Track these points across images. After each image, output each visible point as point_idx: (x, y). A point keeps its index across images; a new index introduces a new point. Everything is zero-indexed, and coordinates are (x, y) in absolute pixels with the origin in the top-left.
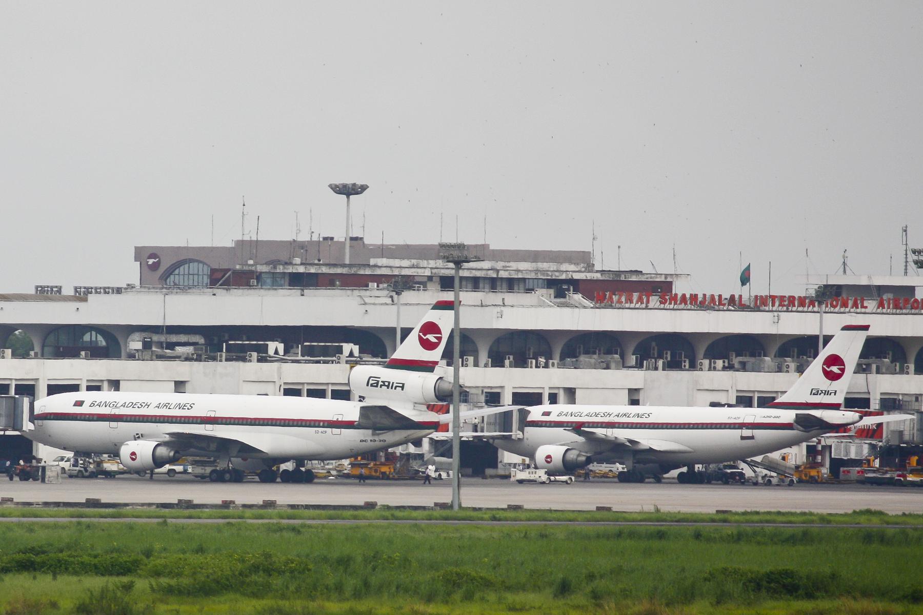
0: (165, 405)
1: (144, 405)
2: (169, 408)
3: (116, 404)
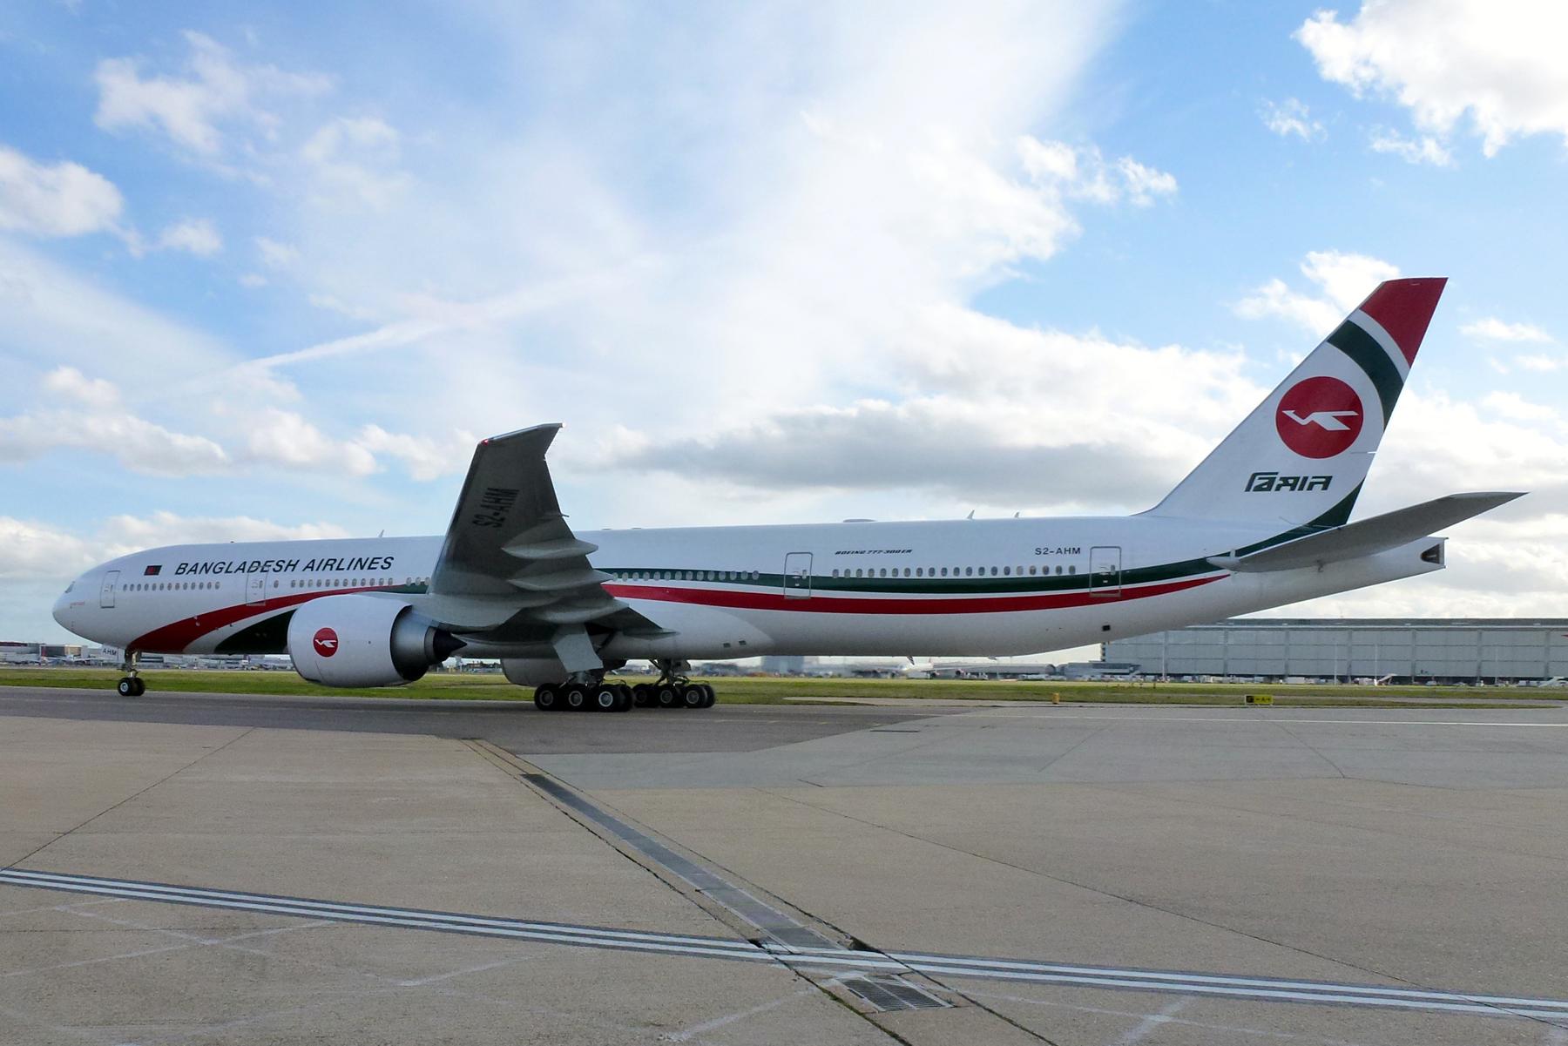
0: (327, 564)
1: (284, 566)
2: (338, 569)
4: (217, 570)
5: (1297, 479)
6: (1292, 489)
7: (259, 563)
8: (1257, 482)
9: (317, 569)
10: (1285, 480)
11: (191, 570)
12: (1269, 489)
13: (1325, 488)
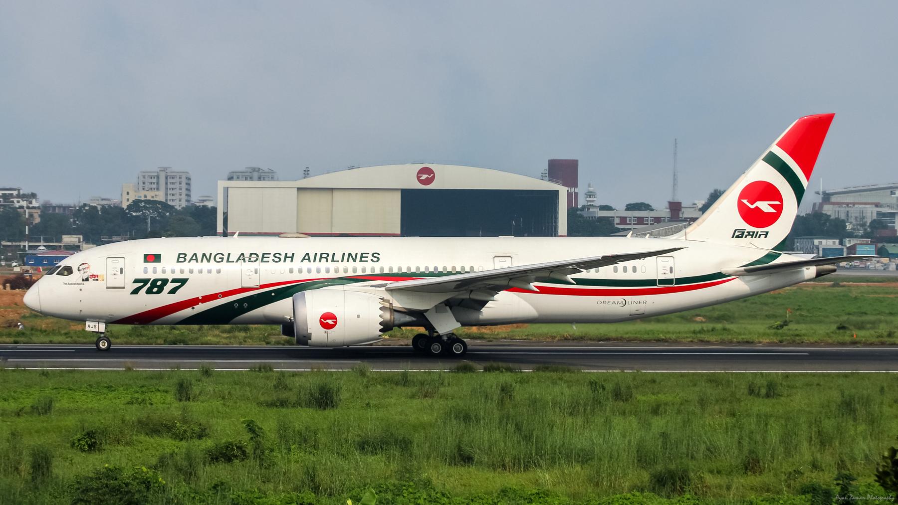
0: (321, 258)
1: (282, 257)
2: (333, 261)
3: (225, 258)
4: (217, 259)
5: (754, 232)
6: (752, 237)
7: (257, 255)
8: (737, 234)
10: (749, 233)
11: (191, 259)
12: (742, 237)
13: (766, 237)
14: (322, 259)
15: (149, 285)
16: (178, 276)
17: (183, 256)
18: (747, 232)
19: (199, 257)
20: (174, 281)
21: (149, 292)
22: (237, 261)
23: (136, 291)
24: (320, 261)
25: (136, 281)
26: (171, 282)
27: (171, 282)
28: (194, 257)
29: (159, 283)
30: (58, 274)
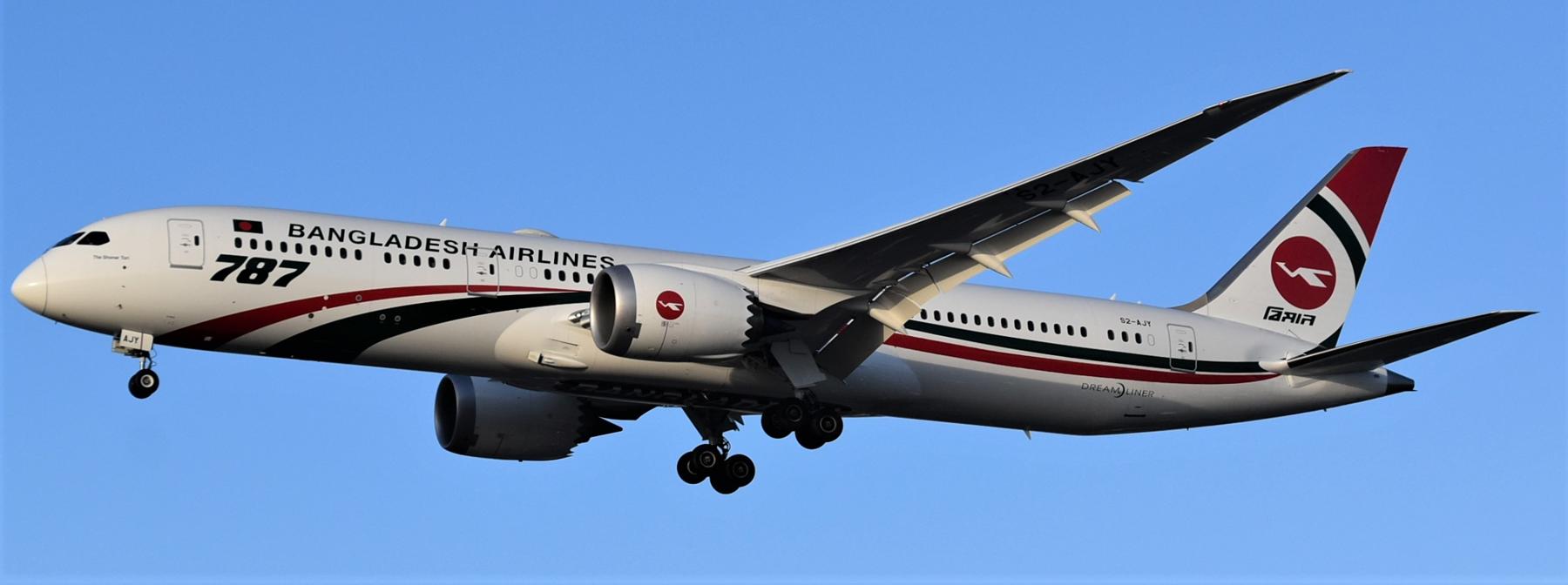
0: (521, 255)
5: (1295, 315)
6: (1292, 321)
9: (511, 257)
10: (1287, 314)
14: (524, 257)
15: (243, 267)
16: (291, 255)
17: (299, 228)
18: (1286, 313)
19: (326, 234)
20: (286, 264)
21: (243, 278)
22: (387, 245)
23: (220, 276)
24: (520, 259)
25: (223, 258)
26: (281, 266)
27: (281, 266)
28: (318, 231)
29: (261, 265)
30: (80, 243)
